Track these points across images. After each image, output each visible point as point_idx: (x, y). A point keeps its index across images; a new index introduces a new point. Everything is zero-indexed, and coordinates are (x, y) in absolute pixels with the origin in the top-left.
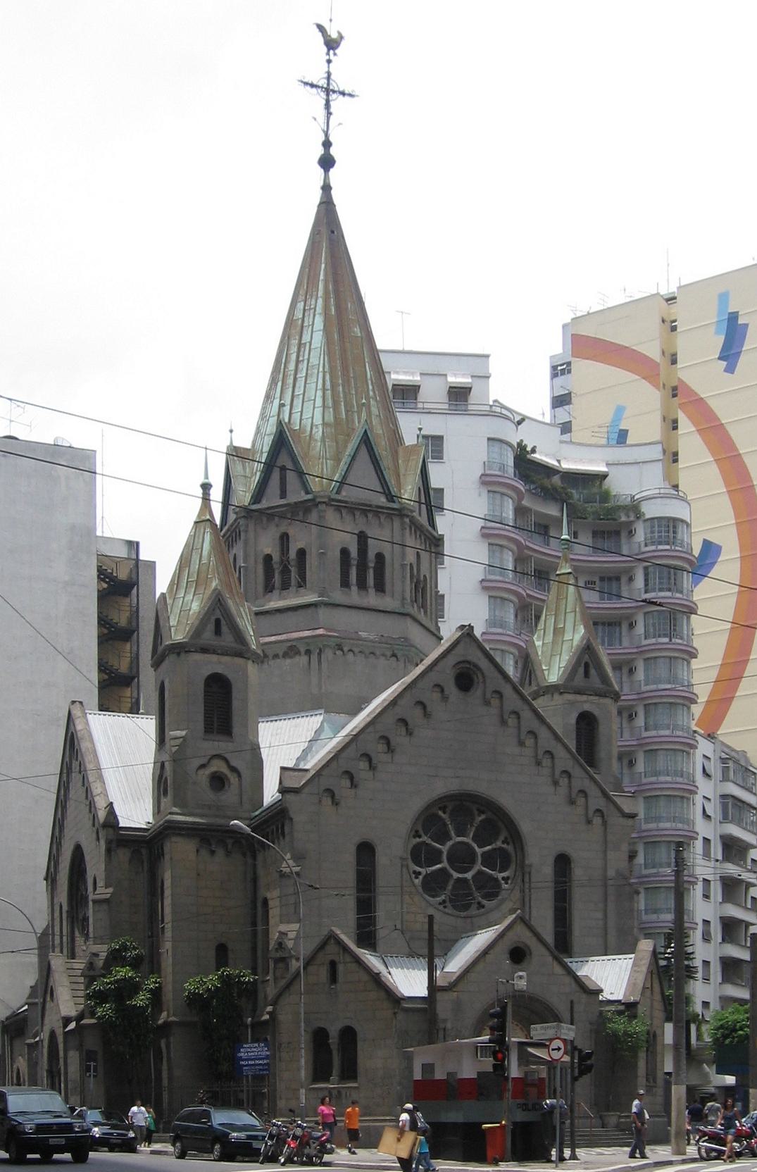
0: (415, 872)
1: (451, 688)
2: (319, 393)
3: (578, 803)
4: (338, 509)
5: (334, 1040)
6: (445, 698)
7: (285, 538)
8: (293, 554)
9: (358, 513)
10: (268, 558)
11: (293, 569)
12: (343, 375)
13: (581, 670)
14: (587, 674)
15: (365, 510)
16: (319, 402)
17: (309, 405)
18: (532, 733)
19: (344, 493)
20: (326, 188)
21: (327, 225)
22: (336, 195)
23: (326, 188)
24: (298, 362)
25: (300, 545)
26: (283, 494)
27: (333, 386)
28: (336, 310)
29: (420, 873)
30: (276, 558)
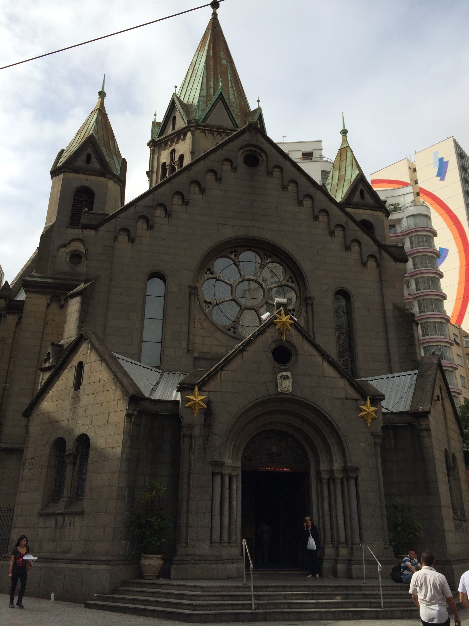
0: (206, 302)
1: (239, 161)
2: (200, 85)
3: (353, 250)
4: (203, 131)
5: (70, 446)
6: (234, 169)
7: (173, 152)
8: (177, 158)
9: (215, 134)
10: (165, 164)
11: (176, 167)
12: (214, 71)
13: (358, 194)
14: (362, 197)
15: (220, 130)
16: (199, 88)
17: (193, 92)
18: (309, 196)
19: (207, 123)
20: (215, 15)
21: (215, 33)
22: (219, 18)
23: (215, 15)
24: (191, 77)
25: (181, 153)
26: (174, 128)
27: (208, 81)
28: (214, 53)
29: (210, 303)
30: (168, 163)
